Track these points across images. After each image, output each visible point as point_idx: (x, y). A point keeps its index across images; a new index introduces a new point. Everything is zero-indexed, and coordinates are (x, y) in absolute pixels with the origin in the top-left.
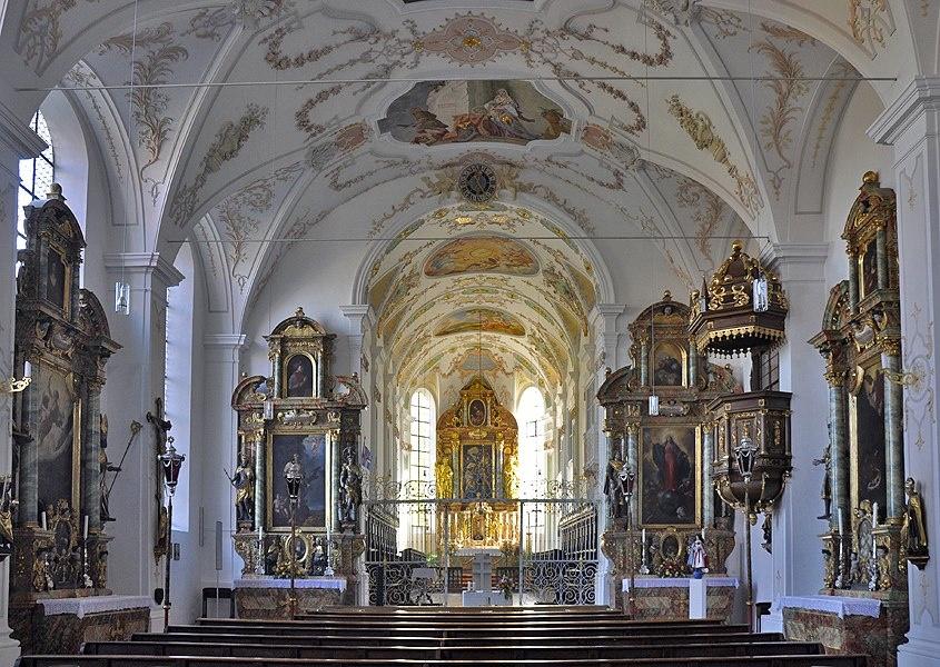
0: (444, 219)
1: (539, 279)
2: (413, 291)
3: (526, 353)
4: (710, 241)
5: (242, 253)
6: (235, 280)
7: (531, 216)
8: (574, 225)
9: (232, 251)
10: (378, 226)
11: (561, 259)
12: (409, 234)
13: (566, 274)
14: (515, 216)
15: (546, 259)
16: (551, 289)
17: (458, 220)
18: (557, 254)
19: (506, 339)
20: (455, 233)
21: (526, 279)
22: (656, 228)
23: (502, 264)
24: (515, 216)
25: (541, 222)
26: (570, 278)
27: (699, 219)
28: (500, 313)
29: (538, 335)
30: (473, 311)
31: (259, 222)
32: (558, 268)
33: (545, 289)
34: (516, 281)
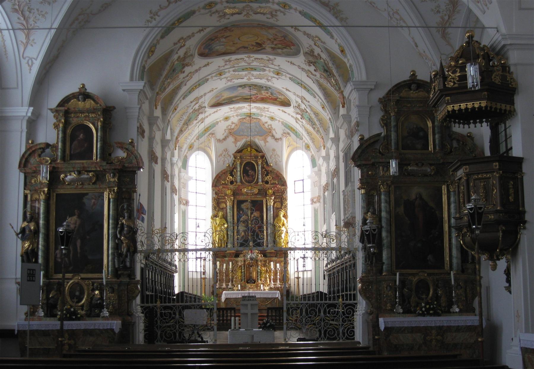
0: (214, 9)
1: (300, 60)
2: (187, 70)
3: (292, 122)
4: (449, 30)
5: (31, 38)
6: (24, 62)
7: (290, 8)
8: (329, 15)
9: (22, 36)
10: (154, 15)
11: (319, 43)
12: (182, 22)
13: (324, 56)
14: (276, 7)
15: (306, 43)
16: (312, 68)
17: (227, 11)
18: (315, 39)
19: (274, 110)
20: (224, 22)
21: (290, 59)
22: (401, 19)
23: (268, 47)
24: (276, 7)
25: (300, 12)
26: (328, 59)
27: (438, 12)
28: (267, 88)
29: (303, 107)
30: (243, 86)
31: (46, 13)
32: (317, 51)
33: (307, 67)
34: (281, 62)
